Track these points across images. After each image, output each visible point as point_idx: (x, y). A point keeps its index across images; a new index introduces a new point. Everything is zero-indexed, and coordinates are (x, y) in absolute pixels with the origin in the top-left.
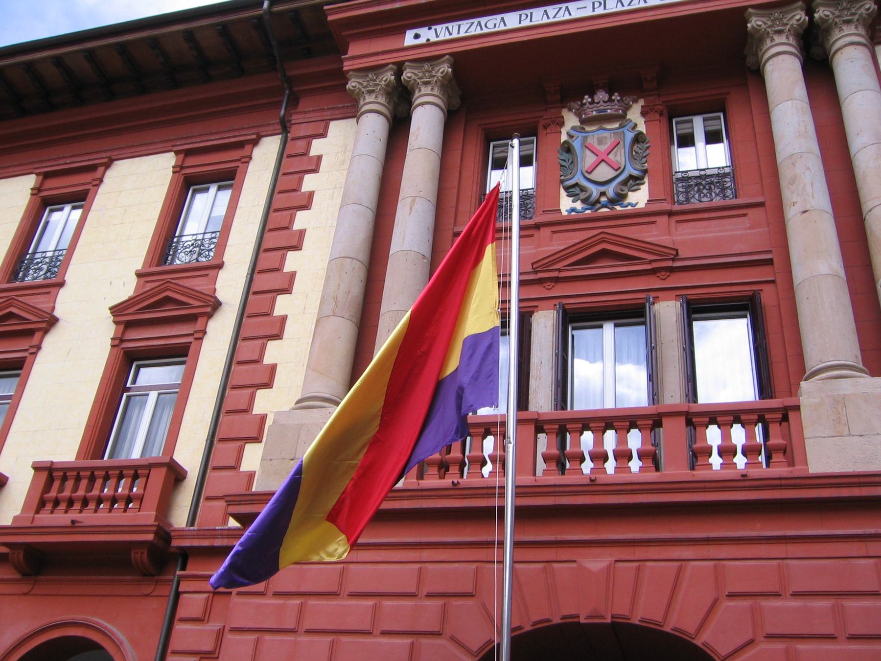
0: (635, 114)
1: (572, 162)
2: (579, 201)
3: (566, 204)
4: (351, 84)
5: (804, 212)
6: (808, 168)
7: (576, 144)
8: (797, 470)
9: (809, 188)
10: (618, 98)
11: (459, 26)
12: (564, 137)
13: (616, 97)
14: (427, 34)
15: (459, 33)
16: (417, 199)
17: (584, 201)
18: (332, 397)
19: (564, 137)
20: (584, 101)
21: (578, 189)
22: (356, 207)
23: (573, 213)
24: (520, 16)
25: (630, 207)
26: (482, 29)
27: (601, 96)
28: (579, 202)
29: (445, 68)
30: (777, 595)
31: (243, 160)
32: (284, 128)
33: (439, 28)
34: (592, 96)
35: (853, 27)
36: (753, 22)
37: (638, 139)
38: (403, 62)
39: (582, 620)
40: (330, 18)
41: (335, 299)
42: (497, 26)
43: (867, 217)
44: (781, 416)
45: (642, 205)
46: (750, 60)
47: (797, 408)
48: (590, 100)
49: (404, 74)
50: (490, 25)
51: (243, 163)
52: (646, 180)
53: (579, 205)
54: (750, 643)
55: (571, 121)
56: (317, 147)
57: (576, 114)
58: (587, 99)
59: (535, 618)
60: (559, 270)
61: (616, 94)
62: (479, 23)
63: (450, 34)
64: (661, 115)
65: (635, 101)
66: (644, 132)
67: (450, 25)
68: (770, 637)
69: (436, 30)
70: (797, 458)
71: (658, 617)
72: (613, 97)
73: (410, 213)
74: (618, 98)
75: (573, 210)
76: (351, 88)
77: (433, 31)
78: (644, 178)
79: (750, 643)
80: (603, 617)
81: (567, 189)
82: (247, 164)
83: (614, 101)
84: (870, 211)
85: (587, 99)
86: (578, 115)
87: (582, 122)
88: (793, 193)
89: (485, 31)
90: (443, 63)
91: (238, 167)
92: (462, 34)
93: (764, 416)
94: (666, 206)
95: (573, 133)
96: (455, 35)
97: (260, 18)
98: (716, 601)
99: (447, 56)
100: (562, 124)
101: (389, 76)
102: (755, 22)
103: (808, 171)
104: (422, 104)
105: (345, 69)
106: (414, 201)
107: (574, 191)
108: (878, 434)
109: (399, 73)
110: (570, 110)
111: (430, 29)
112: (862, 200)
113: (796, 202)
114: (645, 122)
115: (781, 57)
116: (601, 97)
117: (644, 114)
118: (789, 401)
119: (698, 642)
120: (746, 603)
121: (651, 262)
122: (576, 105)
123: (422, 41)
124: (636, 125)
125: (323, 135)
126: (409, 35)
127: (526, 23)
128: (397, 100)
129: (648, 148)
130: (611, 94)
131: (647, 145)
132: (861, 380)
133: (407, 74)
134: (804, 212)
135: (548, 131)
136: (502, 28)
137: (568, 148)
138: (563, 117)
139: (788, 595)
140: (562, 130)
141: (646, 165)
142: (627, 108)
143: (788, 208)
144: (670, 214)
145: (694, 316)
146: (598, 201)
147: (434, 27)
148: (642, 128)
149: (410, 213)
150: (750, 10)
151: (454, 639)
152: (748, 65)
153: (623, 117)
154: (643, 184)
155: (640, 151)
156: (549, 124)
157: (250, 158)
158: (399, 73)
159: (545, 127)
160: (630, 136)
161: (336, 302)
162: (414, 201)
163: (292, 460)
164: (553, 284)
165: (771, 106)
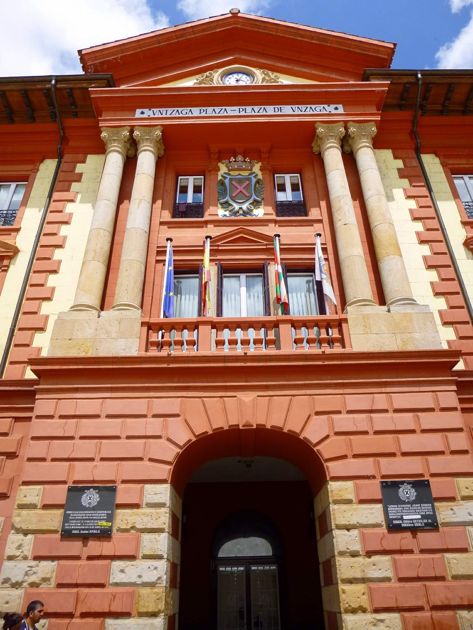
0: (257, 168)
1: (224, 191)
2: (228, 211)
4: (103, 134)
5: (345, 225)
6: (347, 203)
7: (227, 182)
8: (347, 350)
9: (347, 213)
10: (249, 160)
11: (167, 110)
12: (220, 178)
13: (247, 159)
14: (148, 113)
15: (166, 114)
16: (142, 201)
17: (230, 211)
18: (93, 305)
19: (220, 178)
20: (231, 160)
21: (227, 205)
22: (106, 201)
23: (225, 217)
24: (200, 110)
25: (254, 216)
26: (179, 114)
27: (240, 158)
28: (228, 211)
29: (158, 133)
30: (339, 412)
31: (33, 171)
32: (60, 156)
33: (155, 110)
34: (235, 158)
35: (366, 138)
36: (319, 129)
37: (258, 182)
38: (134, 126)
39: (241, 428)
40: (92, 96)
41: (95, 251)
42: (188, 113)
43: (374, 230)
44: (338, 323)
46: (315, 149)
47: (346, 320)
48: (234, 160)
49: (135, 132)
50: (184, 112)
51: (33, 172)
52: (262, 203)
53: (227, 213)
54: (327, 437)
55: (223, 169)
56: (79, 168)
57: (226, 166)
58: (232, 159)
59: (215, 426)
60: (218, 246)
61: (248, 158)
62: (178, 110)
63: (162, 114)
64: (270, 171)
65: (258, 163)
66: (262, 179)
67: (161, 110)
68: (337, 434)
69: (153, 111)
70: (347, 344)
71: (280, 425)
72: (246, 160)
73: (138, 208)
74: (249, 160)
75: (225, 215)
76: (103, 136)
77: (151, 111)
78: (261, 202)
79: (327, 437)
80: (252, 426)
81: (221, 204)
82: (36, 173)
83: (246, 162)
84: (375, 227)
85: (232, 159)
86: (228, 167)
87: (229, 170)
88: (339, 215)
89: (181, 115)
90: (157, 129)
91: (30, 174)
92: (168, 116)
93: (329, 323)
94: (274, 217)
95: (225, 175)
96: (164, 116)
97: (49, 90)
98: (309, 416)
99: (159, 126)
100: (218, 170)
101: (126, 133)
102: (320, 130)
103: (346, 205)
104: (145, 150)
105: (100, 125)
106: (140, 201)
108: (384, 333)
109: (132, 132)
110: (223, 163)
111: (150, 110)
112: (371, 222)
113: (341, 219)
114: (262, 174)
115: (332, 149)
116: (240, 159)
117: (261, 169)
118: (343, 316)
119: (301, 437)
120: (325, 417)
121: (266, 245)
122: (227, 161)
124: (257, 175)
125: (84, 162)
126: (138, 111)
128: (129, 147)
129: (263, 187)
130: (245, 158)
131: (263, 186)
132: (375, 307)
133: (136, 133)
134: (345, 225)
135: (212, 173)
136: (190, 115)
137: (222, 183)
138: (219, 167)
139: (345, 412)
140: (218, 174)
141: (262, 196)
143: (337, 222)
144: (275, 222)
145: (288, 274)
146: (238, 212)
147: (152, 109)
148: (260, 176)
149: (138, 208)
150: (318, 123)
151: (169, 440)
152: (314, 151)
153: (251, 170)
154: (262, 205)
155: (260, 189)
156: (212, 170)
157: (38, 170)
158: (132, 132)
159: (209, 171)
160: (254, 180)
161: (95, 253)
162: (140, 201)
163: (70, 340)
164: (215, 253)
165: (327, 172)
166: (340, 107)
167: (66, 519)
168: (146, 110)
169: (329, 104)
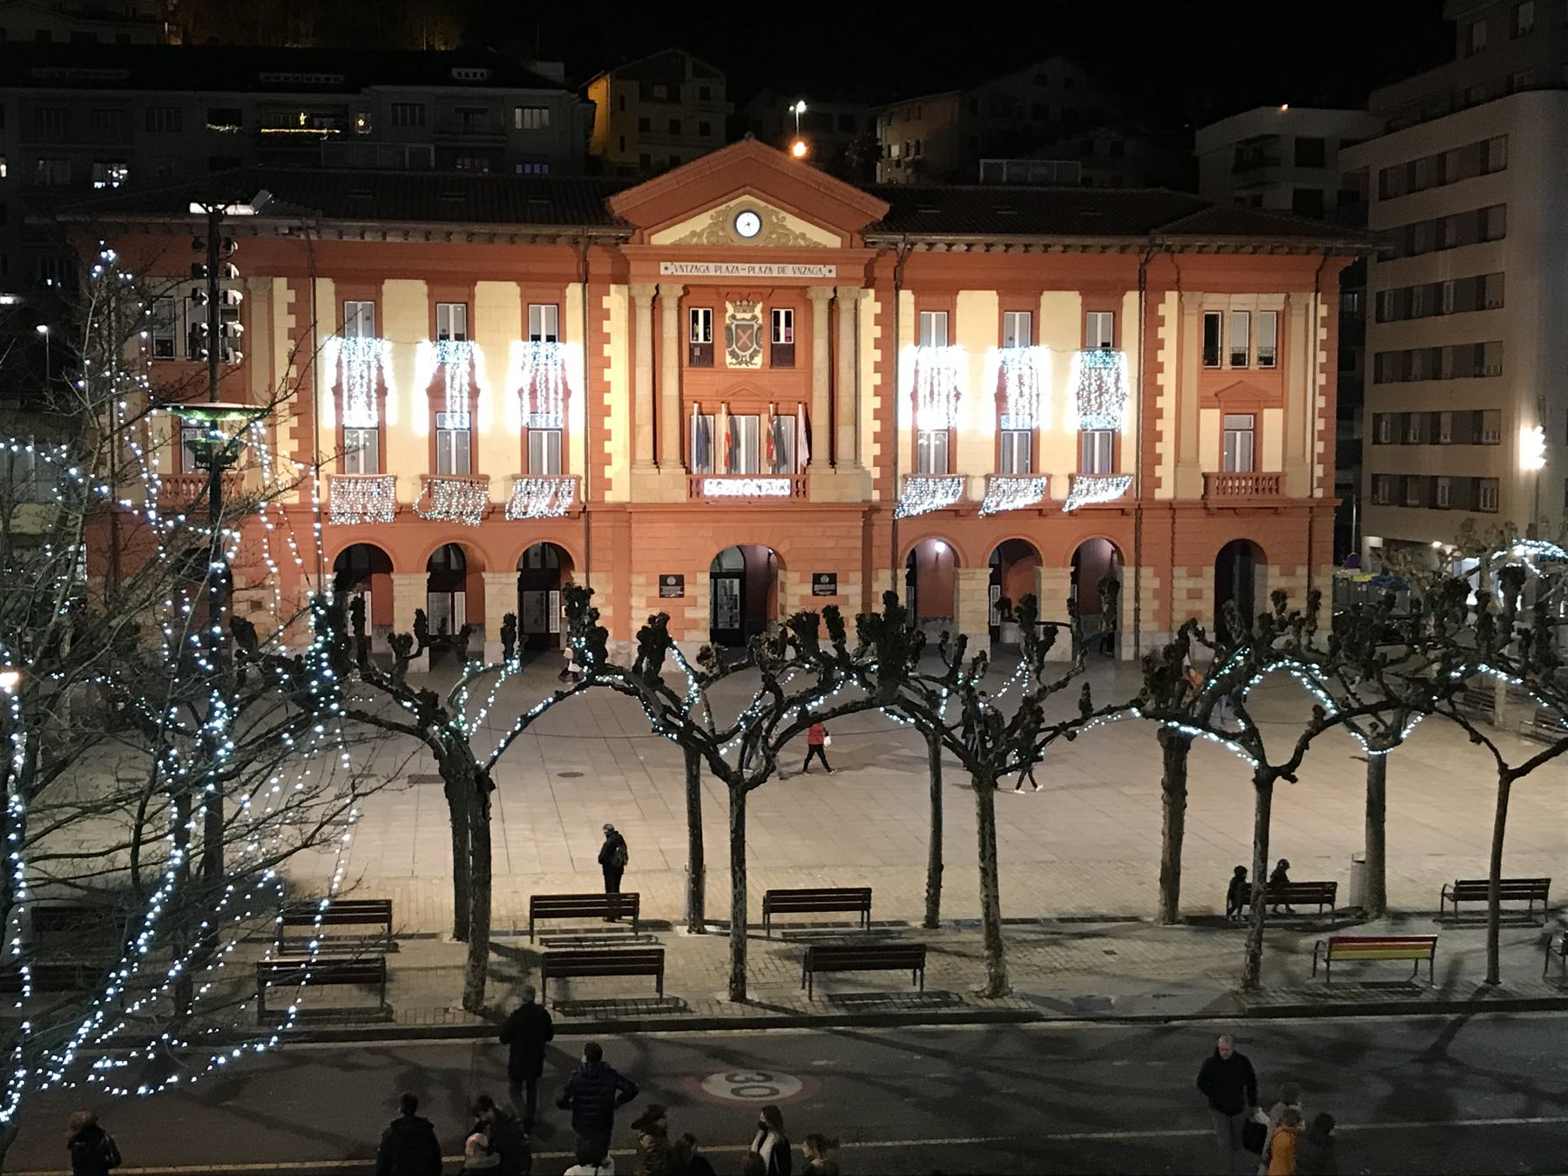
3: (729, 359)
7: (733, 327)
12: (728, 321)
33: (678, 264)
45: (758, 367)
56: (607, 302)
100: (725, 311)
107: (733, 354)
117: (762, 311)
123: (668, 272)
125: (608, 294)
126: (663, 265)
127: (718, 274)
137: (728, 328)
142: (754, 306)
148: (760, 322)
160: (756, 328)
166: (833, 268)
167: (661, 590)
168: (668, 264)
169: (824, 264)
